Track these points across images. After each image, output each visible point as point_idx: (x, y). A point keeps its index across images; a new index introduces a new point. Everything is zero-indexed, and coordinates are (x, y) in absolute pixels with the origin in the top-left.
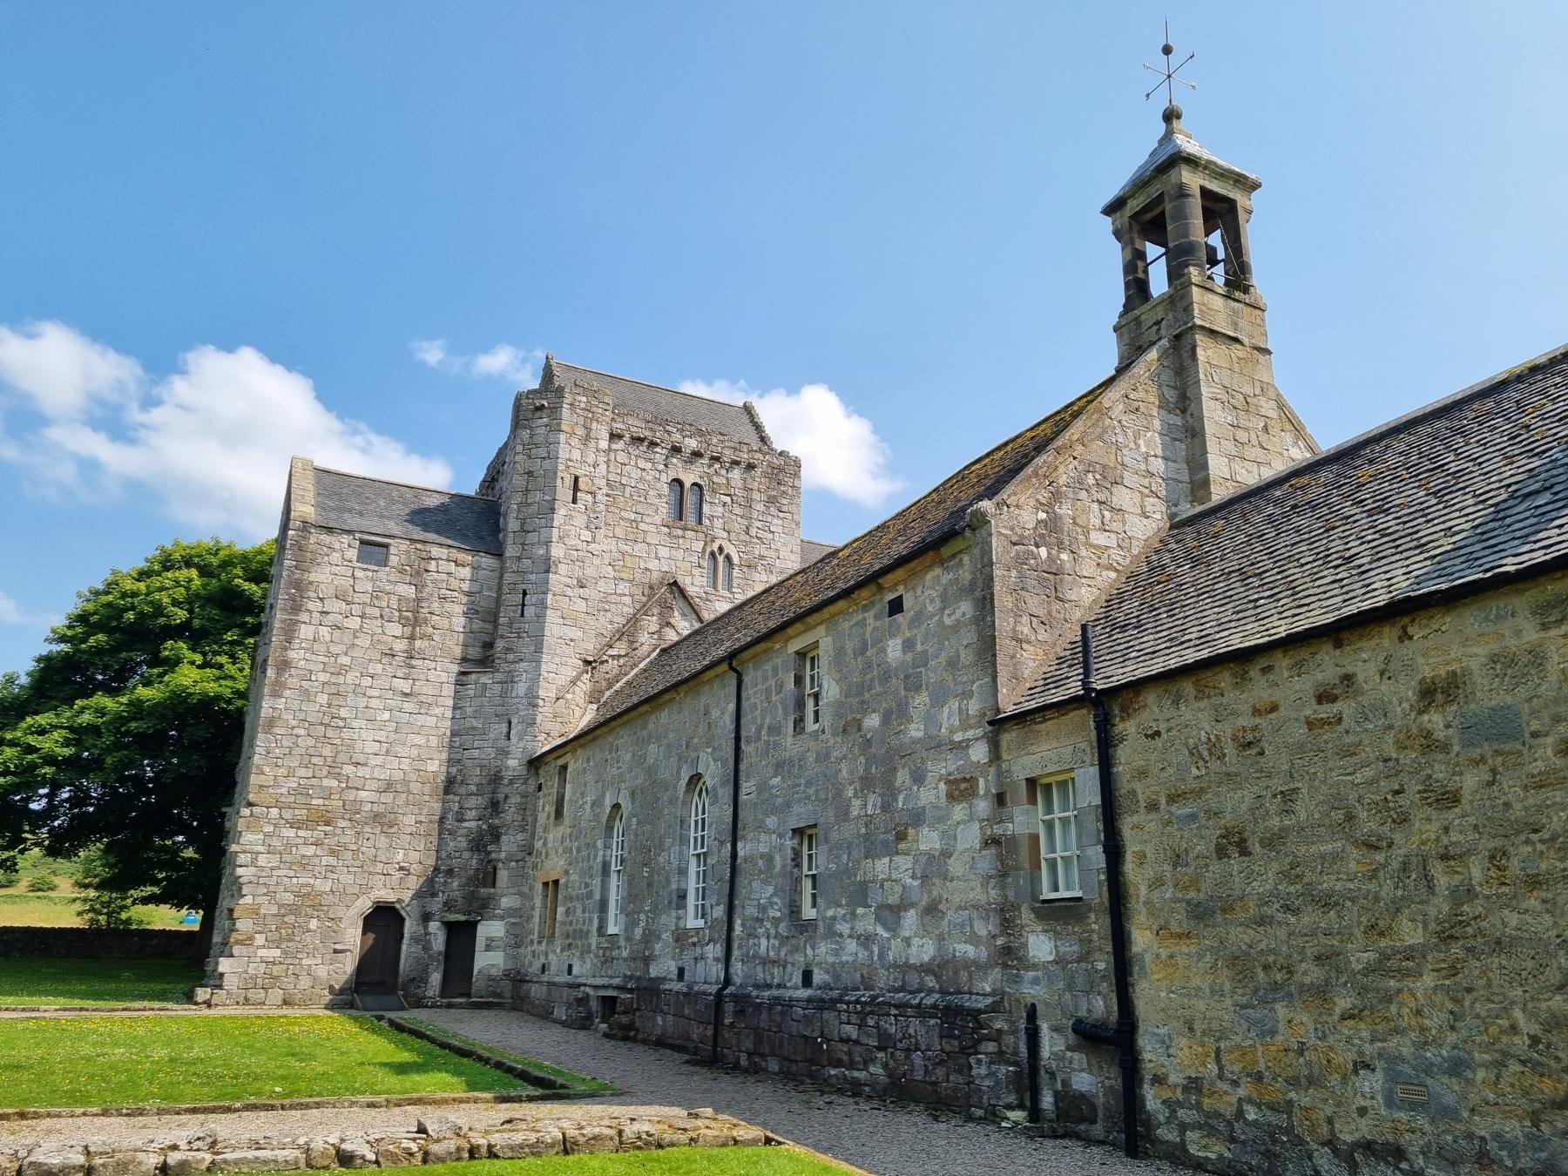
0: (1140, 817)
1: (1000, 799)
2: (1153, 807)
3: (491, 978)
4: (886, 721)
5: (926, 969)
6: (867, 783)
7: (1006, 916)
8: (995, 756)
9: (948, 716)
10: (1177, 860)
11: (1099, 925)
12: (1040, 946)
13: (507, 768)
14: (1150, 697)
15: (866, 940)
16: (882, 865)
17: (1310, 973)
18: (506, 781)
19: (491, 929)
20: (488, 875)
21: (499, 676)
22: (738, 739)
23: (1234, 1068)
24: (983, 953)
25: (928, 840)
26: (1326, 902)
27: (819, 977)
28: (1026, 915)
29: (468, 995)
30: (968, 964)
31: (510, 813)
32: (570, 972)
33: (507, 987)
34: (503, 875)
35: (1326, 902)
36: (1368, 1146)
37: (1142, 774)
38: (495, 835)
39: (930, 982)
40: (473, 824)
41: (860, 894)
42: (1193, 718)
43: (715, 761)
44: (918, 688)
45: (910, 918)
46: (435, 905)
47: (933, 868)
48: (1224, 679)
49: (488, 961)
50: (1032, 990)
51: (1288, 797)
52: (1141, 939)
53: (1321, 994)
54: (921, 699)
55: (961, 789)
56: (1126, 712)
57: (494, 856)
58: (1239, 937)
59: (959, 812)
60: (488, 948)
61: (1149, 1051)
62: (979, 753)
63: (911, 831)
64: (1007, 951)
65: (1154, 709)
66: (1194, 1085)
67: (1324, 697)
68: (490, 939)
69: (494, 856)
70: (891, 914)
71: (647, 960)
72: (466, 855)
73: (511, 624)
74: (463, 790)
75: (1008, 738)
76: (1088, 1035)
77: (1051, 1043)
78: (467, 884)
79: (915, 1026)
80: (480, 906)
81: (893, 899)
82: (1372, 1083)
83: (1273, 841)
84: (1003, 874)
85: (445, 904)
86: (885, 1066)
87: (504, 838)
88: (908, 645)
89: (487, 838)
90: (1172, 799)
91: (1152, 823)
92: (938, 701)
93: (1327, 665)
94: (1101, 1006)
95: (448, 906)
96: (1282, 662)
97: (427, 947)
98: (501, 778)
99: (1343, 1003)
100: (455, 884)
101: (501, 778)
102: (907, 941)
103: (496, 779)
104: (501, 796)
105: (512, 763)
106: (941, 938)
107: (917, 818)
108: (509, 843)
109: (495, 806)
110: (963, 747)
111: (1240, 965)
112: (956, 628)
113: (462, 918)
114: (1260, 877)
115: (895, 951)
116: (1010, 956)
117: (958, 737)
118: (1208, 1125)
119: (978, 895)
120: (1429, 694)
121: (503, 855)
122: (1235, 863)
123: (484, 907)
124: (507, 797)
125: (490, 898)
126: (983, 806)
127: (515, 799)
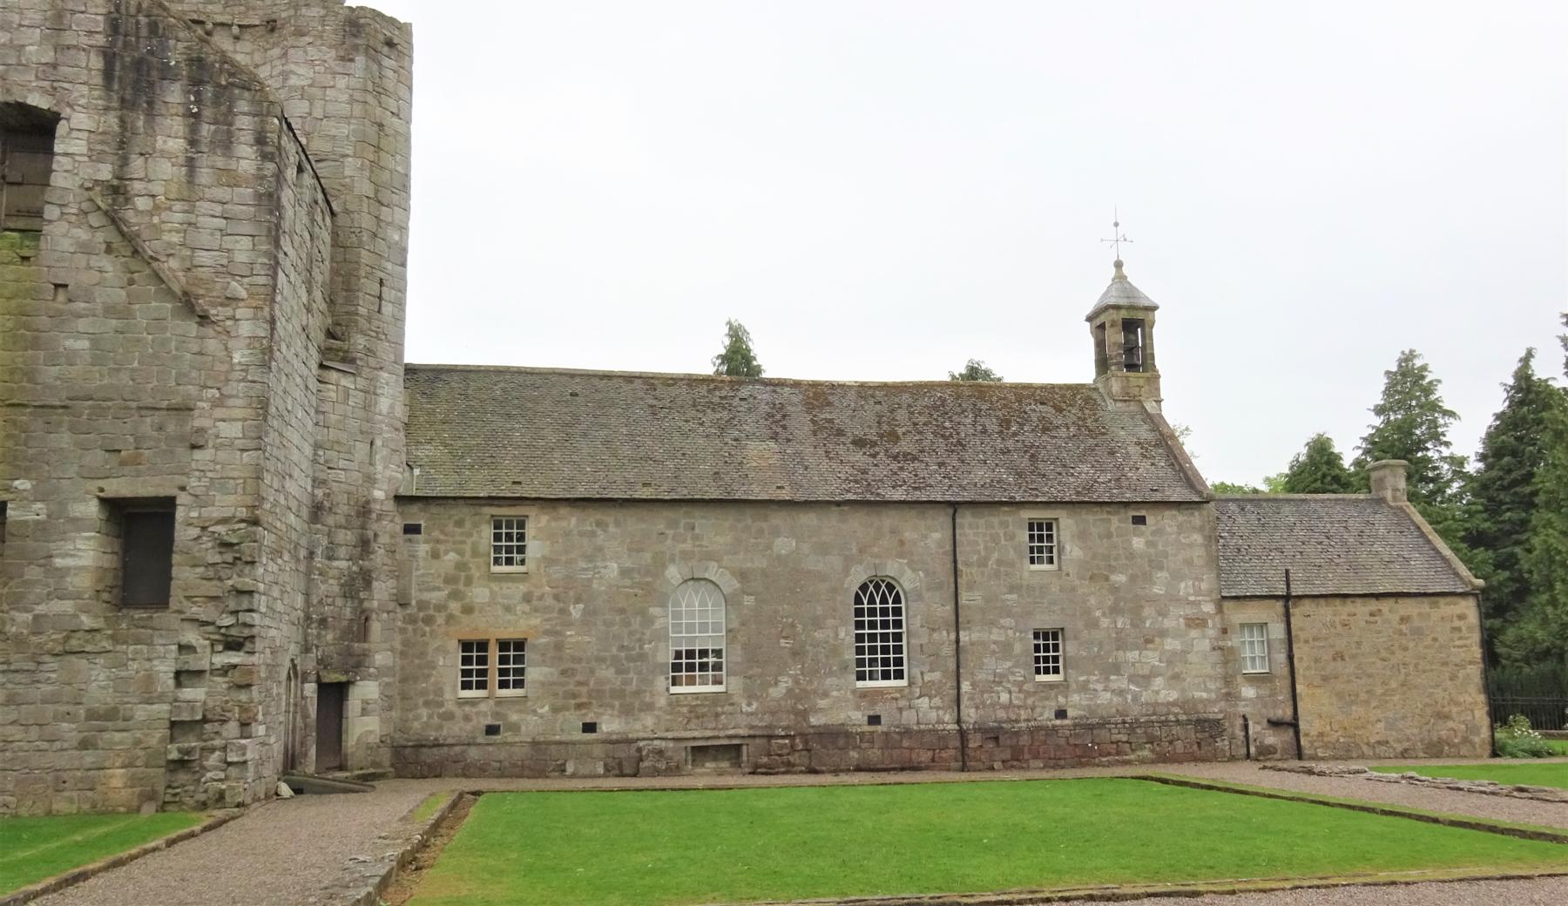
0: (1301, 644)
1: (1225, 631)
2: (1306, 642)
3: (369, 747)
4: (1133, 579)
5: (1174, 704)
6: (1115, 610)
7: (1228, 680)
8: (1220, 610)
9: (1184, 587)
10: (1317, 661)
11: (1282, 685)
12: (1249, 692)
13: (375, 500)
14: (1307, 602)
15: (1121, 693)
16: (1133, 655)
17: (1363, 696)
18: (374, 516)
19: (365, 691)
20: (360, 627)
21: (361, 382)
22: (955, 562)
23: (1336, 727)
24: (1213, 696)
25: (1171, 644)
26: (1370, 676)
27: (1070, 713)
28: (1239, 679)
29: (341, 768)
30: (1201, 700)
31: (379, 556)
32: (590, 728)
33: (385, 756)
34: (376, 627)
35: (1370, 676)
36: (1379, 742)
37: (1302, 629)
38: (366, 578)
39: (1176, 710)
40: (343, 564)
41: (1116, 668)
42: (1325, 612)
43: (914, 570)
44: (1161, 568)
45: (1158, 682)
46: (309, 664)
47: (1172, 659)
48: (1338, 601)
49: (365, 725)
50: (1242, 709)
51: (1359, 644)
52: (1299, 688)
53: (1367, 702)
54: (1162, 575)
55: (1197, 622)
56: (1295, 606)
57: (366, 604)
58: (1340, 686)
59: (1194, 633)
60: (364, 712)
61: (1302, 725)
62: (1209, 608)
63: (1157, 640)
64: (1228, 694)
65: (1307, 606)
66: (1321, 734)
67: (1372, 615)
68: (366, 702)
69: (366, 604)
70: (1145, 680)
71: (804, 714)
72: (339, 602)
73: (369, 320)
74: (330, 520)
75: (1226, 604)
76: (1275, 724)
77: (1253, 729)
78: (342, 638)
79: (1176, 730)
80: (357, 664)
81: (1146, 672)
82: (1381, 725)
83: (1353, 657)
84: (1226, 663)
85: (320, 662)
86: (1152, 751)
87: (375, 584)
88: (1150, 544)
89: (359, 583)
90: (1315, 639)
91: (1306, 648)
92: (1177, 576)
93: (1373, 605)
94: (1285, 713)
95: (322, 663)
96: (1359, 601)
97: (305, 716)
98: (370, 512)
99: (1374, 704)
100: (330, 637)
101: (370, 512)
102: (1157, 692)
103: (364, 510)
104: (370, 534)
105: (379, 494)
106: (1183, 690)
107: (1163, 633)
108: (382, 590)
109: (365, 545)
110: (1197, 604)
111: (1340, 696)
112: (1191, 546)
113: (343, 679)
114: (1349, 668)
115: (1145, 697)
116: (1231, 696)
117: (1192, 598)
118: (1326, 746)
119: (1208, 670)
120: (1403, 620)
121: (375, 604)
122: (1339, 663)
123: (358, 665)
124: (376, 535)
125: (365, 654)
126: (1211, 633)
127: (384, 539)
